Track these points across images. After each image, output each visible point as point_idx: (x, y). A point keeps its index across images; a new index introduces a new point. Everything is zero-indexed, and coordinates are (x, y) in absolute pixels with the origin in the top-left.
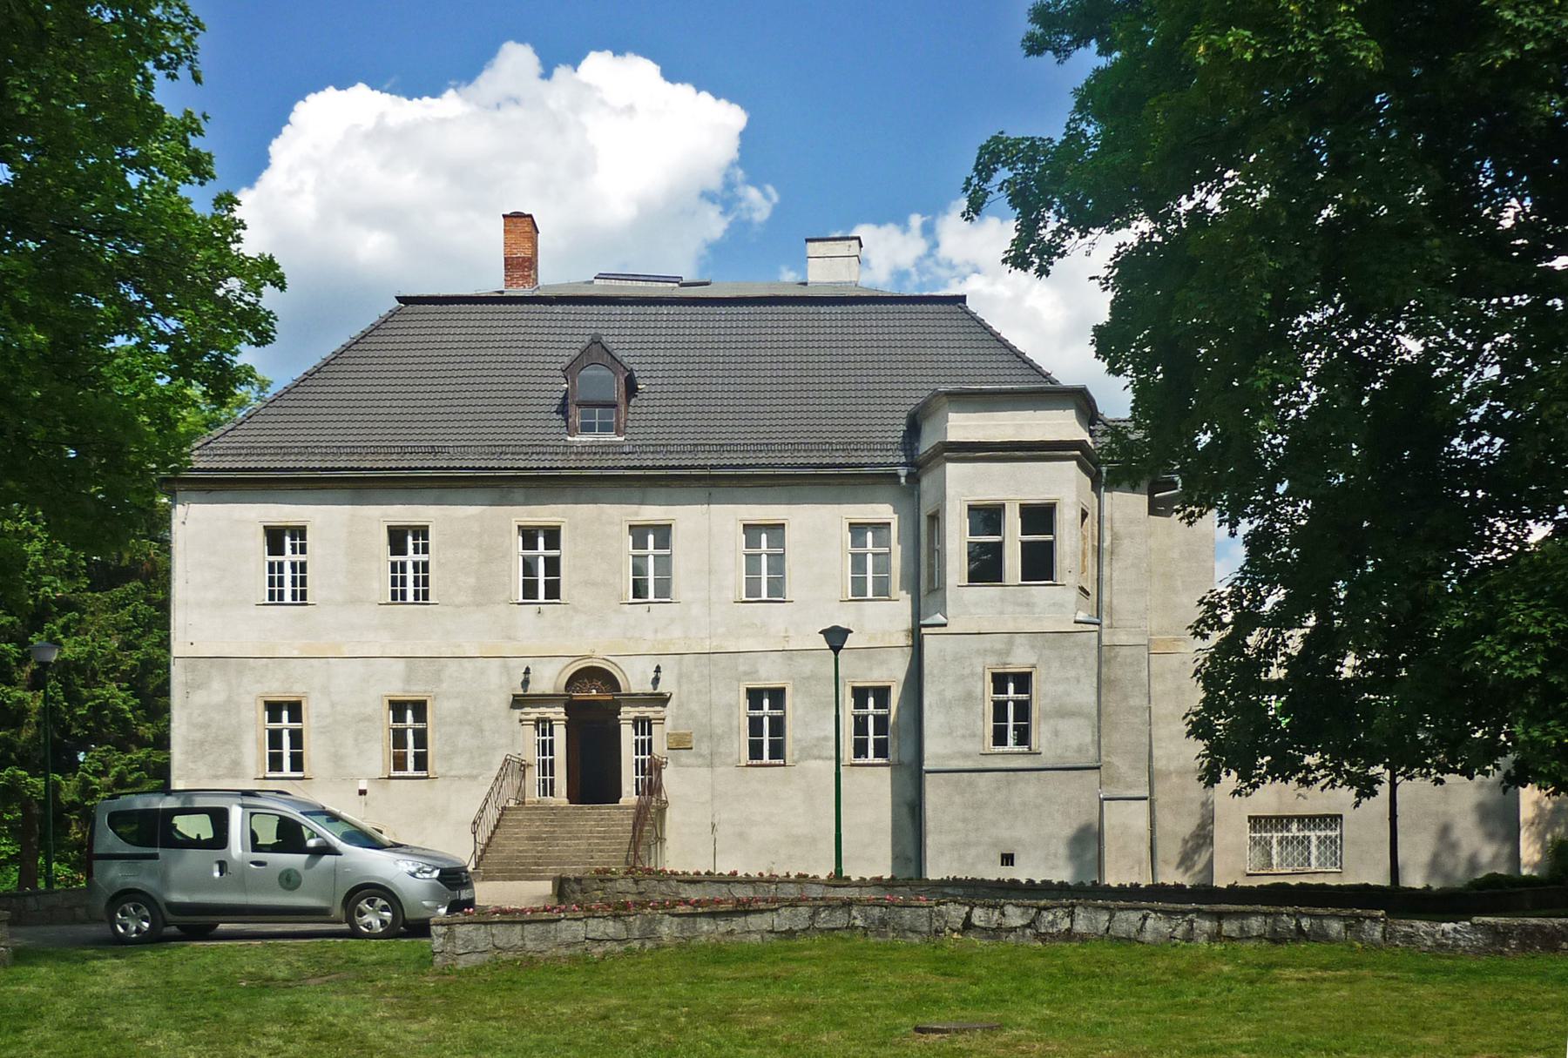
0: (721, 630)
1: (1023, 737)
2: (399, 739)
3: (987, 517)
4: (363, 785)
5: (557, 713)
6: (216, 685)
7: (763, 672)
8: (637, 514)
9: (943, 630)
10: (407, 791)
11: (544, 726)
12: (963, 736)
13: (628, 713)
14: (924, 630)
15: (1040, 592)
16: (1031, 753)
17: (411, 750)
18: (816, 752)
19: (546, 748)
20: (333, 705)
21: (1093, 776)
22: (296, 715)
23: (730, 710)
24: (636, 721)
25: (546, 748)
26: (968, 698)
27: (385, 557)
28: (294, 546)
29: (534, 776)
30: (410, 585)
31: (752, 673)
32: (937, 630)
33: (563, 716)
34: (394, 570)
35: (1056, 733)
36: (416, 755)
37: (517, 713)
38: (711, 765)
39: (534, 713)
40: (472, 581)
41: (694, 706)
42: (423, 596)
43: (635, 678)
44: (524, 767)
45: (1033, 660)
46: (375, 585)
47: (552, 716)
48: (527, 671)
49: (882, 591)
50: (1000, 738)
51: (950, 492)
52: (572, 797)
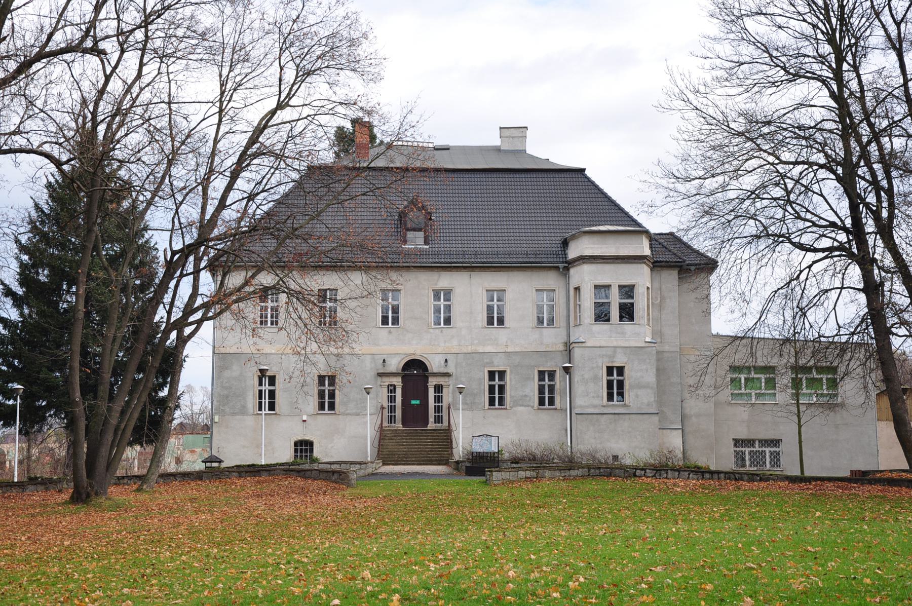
0: (476, 342)
2: (321, 394)
4: (305, 418)
5: (398, 381)
6: (235, 367)
9: (583, 345)
10: (326, 420)
11: (392, 389)
13: (432, 382)
15: (628, 326)
16: (625, 406)
18: (521, 403)
19: (392, 399)
21: (656, 419)
25: (392, 399)
26: (595, 378)
31: (491, 363)
32: (580, 345)
35: (637, 396)
38: (471, 409)
43: (435, 364)
44: (383, 408)
45: (626, 360)
48: (384, 361)
51: (586, 279)
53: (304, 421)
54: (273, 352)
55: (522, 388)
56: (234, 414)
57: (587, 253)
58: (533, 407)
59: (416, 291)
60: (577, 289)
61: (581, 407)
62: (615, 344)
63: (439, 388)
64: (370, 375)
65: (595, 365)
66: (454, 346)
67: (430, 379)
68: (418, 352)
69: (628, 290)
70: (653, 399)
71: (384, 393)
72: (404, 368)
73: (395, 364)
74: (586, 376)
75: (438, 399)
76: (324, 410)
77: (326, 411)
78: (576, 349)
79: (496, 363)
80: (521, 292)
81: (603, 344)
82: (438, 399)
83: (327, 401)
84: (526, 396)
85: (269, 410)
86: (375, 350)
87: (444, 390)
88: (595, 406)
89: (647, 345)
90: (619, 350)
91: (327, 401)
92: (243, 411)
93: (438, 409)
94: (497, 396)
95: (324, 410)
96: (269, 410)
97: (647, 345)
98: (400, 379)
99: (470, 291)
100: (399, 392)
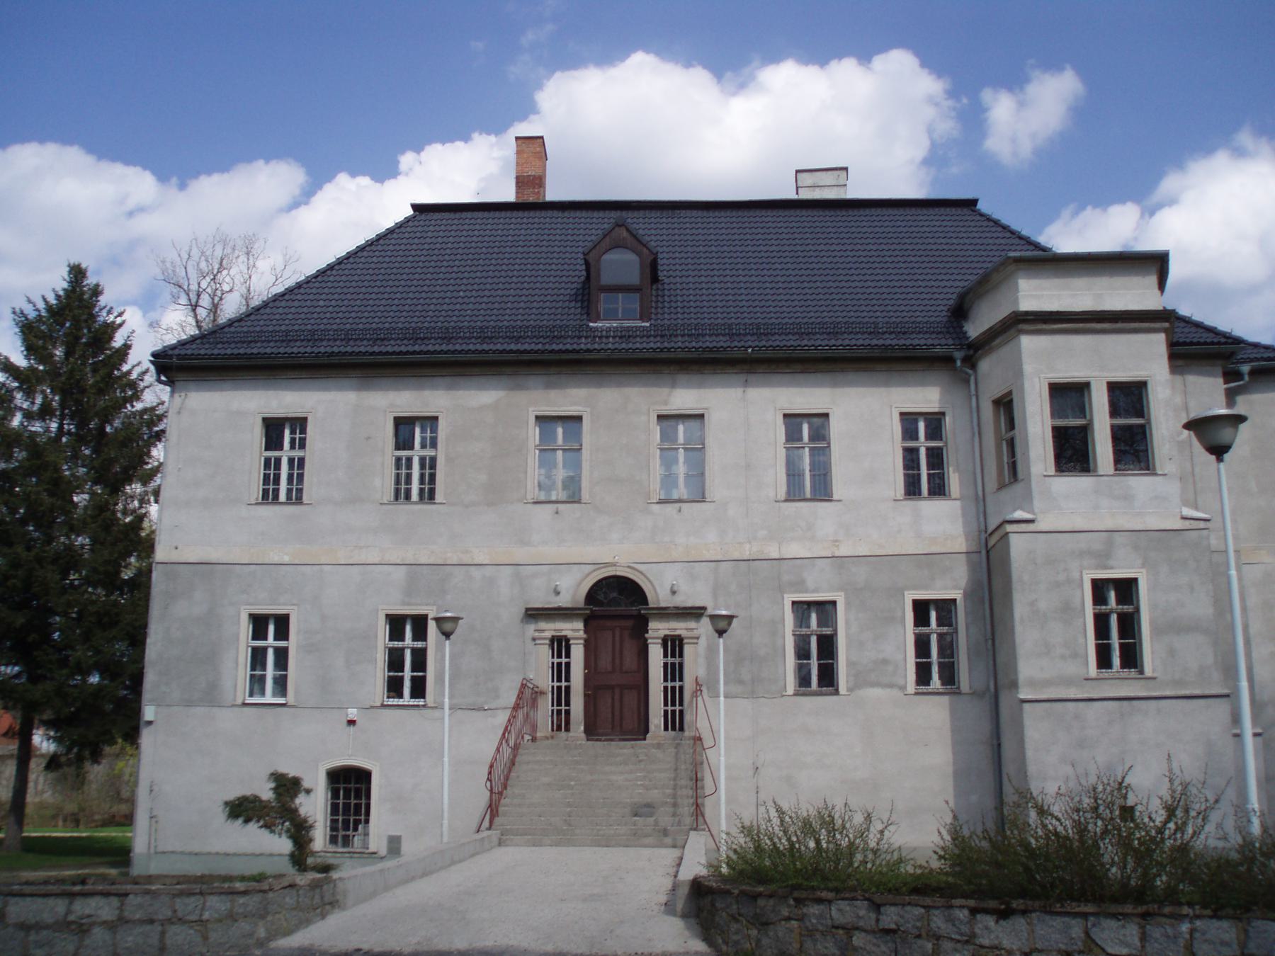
0: (762, 533)
1: (1131, 658)
2: (395, 661)
3: (1069, 395)
4: (353, 713)
5: (574, 629)
7: (811, 578)
8: (666, 403)
9: (1031, 527)
11: (560, 645)
12: (1063, 657)
13: (658, 629)
14: (1009, 528)
15: (1138, 483)
17: (407, 674)
19: (562, 672)
22: (282, 633)
23: (775, 627)
24: (665, 641)
25: (562, 672)
27: (389, 452)
28: (293, 441)
29: (546, 706)
30: (417, 482)
31: (799, 585)
32: (1023, 527)
33: (581, 634)
34: (398, 466)
35: (1172, 652)
36: (413, 679)
37: (531, 629)
38: (753, 695)
39: (551, 628)
42: (428, 495)
44: (537, 693)
46: (377, 482)
47: (569, 634)
49: (938, 489)
50: (1104, 660)
51: (1028, 368)
52: (592, 731)
53: (352, 723)
54: (286, 559)
55: (878, 644)
56: (189, 703)
57: (1026, 305)
58: (903, 688)
59: (617, 414)
60: (1006, 405)
61: (1032, 683)
62: (1109, 524)
63: (674, 645)
65: (1061, 577)
66: (711, 543)
67: (652, 625)
68: (623, 559)
69: (1129, 397)
70: (1210, 660)
71: (544, 656)
72: (591, 596)
74: (1042, 605)
75: (674, 672)
76: (400, 696)
77: (407, 699)
78: (1014, 539)
79: (810, 583)
80: (867, 418)
81: (1080, 524)
82: (674, 672)
83: (406, 678)
84: (885, 662)
85: (413, 696)
86: (520, 554)
87: (688, 649)
88: (1068, 682)
89: (1187, 524)
90: (1118, 538)
91: (406, 678)
92: (211, 697)
93: (674, 696)
94: (820, 666)
95: (400, 696)
96: (413, 696)
97: (1187, 524)
98: (580, 625)
99: (745, 418)
100: (578, 653)
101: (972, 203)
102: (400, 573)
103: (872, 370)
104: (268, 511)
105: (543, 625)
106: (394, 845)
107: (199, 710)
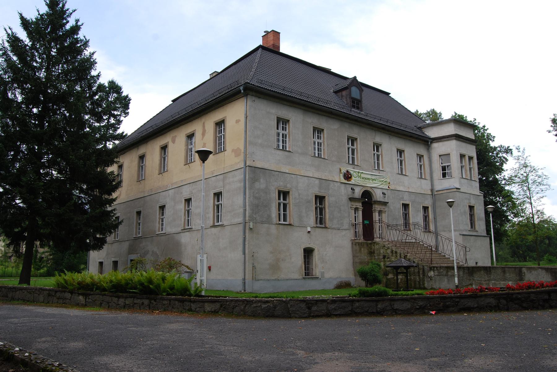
4: (309, 229)
5: (359, 205)
6: (262, 180)
11: (356, 209)
13: (377, 207)
20: (299, 195)
31: (402, 198)
37: (350, 203)
40: (336, 153)
41: (392, 208)
43: (378, 195)
53: (309, 232)
54: (287, 171)
56: (262, 223)
63: (380, 212)
64: (345, 199)
73: (358, 192)
79: (405, 199)
92: (268, 221)
98: (361, 205)
100: (360, 213)
101: (388, 94)
102: (317, 182)
103: (407, 139)
104: (278, 152)
105: (353, 203)
106: (323, 273)
107: (266, 225)
